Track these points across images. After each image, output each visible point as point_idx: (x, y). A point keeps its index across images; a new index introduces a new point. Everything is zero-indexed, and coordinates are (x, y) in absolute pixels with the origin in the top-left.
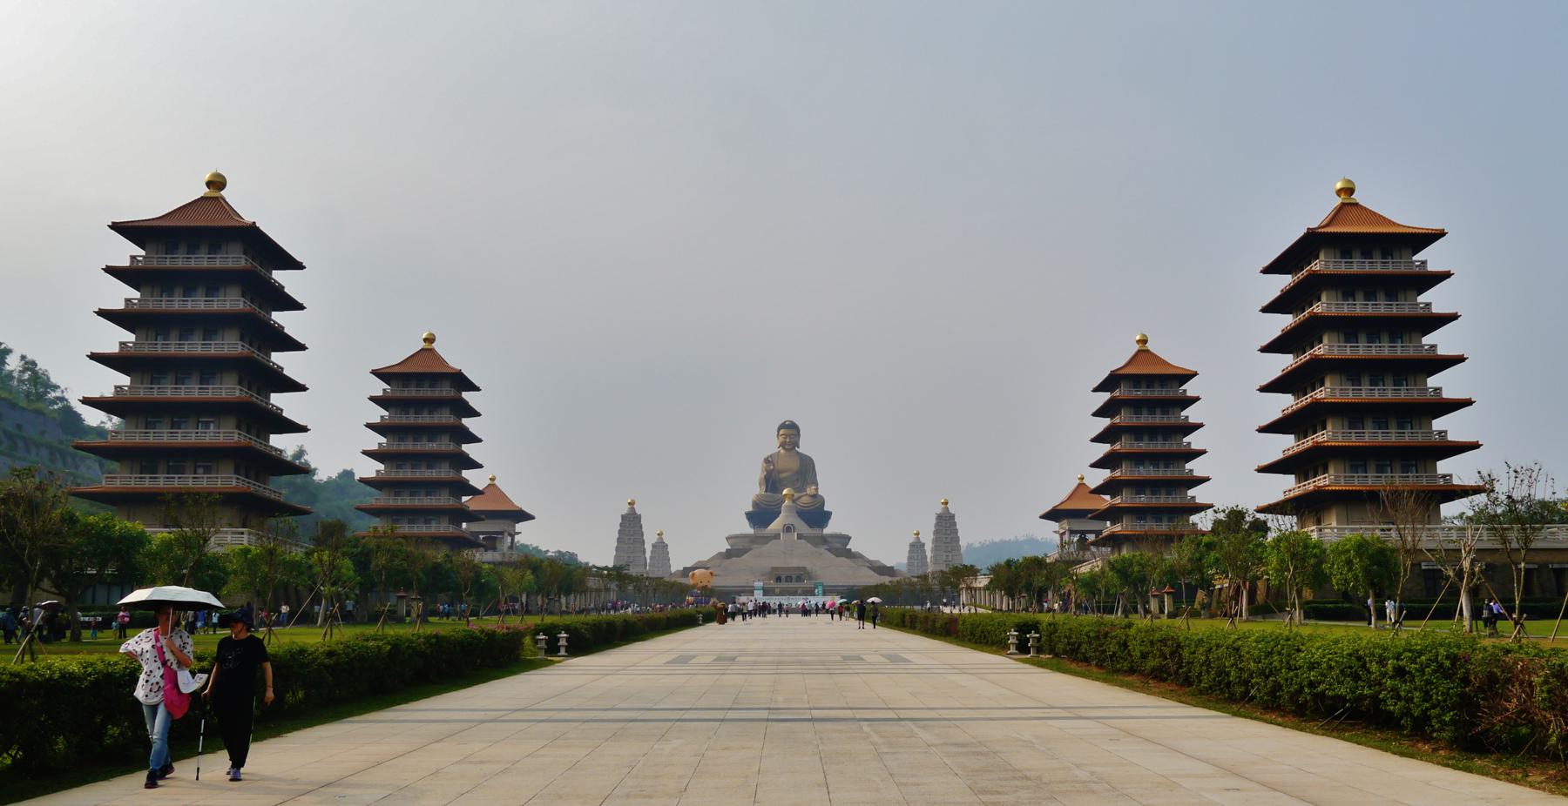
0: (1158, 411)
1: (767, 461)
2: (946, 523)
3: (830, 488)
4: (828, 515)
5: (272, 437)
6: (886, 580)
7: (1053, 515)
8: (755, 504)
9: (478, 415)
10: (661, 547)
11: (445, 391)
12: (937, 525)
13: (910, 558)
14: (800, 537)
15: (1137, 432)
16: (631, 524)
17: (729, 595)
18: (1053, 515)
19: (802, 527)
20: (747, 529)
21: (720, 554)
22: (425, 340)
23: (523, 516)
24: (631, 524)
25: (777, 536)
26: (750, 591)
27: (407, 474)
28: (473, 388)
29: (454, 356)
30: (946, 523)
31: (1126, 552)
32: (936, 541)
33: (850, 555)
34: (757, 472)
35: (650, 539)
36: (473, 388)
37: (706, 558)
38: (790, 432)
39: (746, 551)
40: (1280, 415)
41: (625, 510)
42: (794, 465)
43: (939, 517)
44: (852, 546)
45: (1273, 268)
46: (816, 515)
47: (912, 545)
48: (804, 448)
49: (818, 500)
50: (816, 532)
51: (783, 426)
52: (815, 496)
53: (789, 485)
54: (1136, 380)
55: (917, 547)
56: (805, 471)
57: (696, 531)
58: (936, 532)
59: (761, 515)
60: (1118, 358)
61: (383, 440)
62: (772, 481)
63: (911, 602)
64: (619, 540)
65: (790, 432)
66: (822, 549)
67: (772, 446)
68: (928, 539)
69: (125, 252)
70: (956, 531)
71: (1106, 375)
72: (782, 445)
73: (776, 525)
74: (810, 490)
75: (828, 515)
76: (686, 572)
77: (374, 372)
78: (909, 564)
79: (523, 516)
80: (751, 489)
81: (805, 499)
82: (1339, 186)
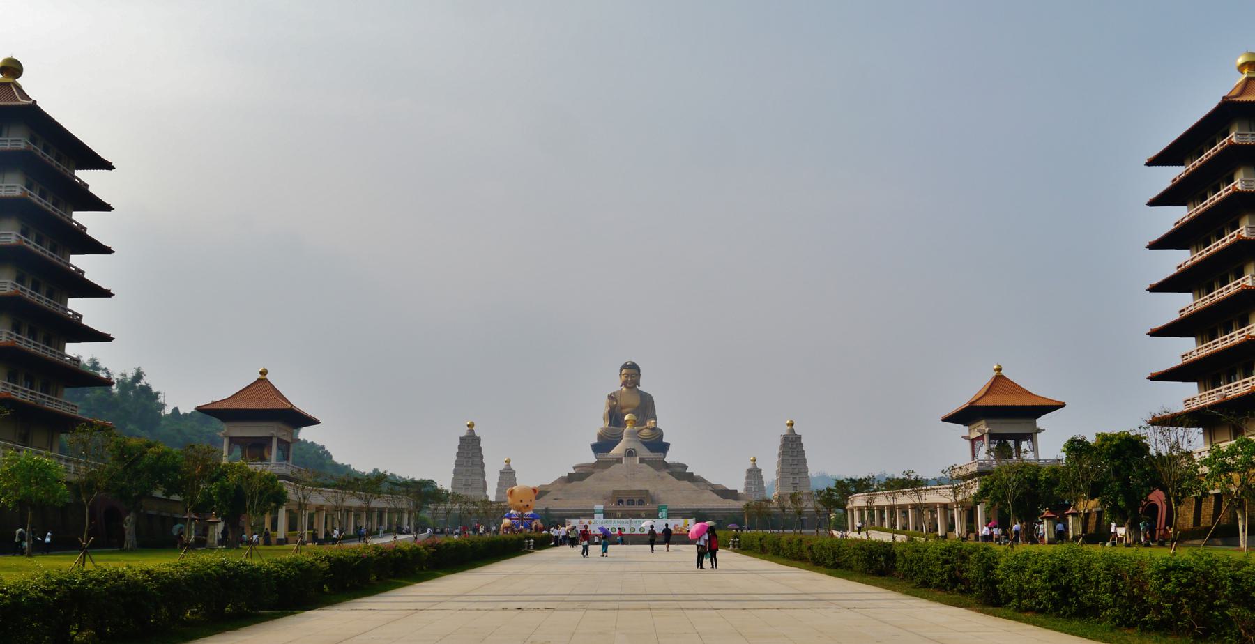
1: (611, 397)
2: (792, 446)
3: (667, 421)
7: (964, 416)
8: (600, 437)
14: (642, 461)
17: (557, 519)
18: (964, 416)
19: (645, 453)
20: (591, 458)
21: (562, 478)
25: (619, 461)
26: (590, 514)
30: (792, 446)
33: (691, 477)
34: (603, 408)
37: (548, 482)
38: (632, 372)
39: (587, 475)
40: (1177, 316)
41: (464, 432)
42: (636, 401)
45: (1162, 159)
47: (749, 471)
48: (644, 386)
50: (657, 456)
51: (625, 366)
52: (654, 429)
55: (754, 474)
56: (646, 407)
57: (539, 453)
59: (603, 445)
62: (615, 416)
63: (796, 526)
65: (632, 372)
66: (665, 473)
70: (803, 453)
71: (1219, 100)
72: (625, 384)
73: (618, 450)
74: (650, 423)
80: (597, 423)
81: (645, 432)
82: (1241, 60)
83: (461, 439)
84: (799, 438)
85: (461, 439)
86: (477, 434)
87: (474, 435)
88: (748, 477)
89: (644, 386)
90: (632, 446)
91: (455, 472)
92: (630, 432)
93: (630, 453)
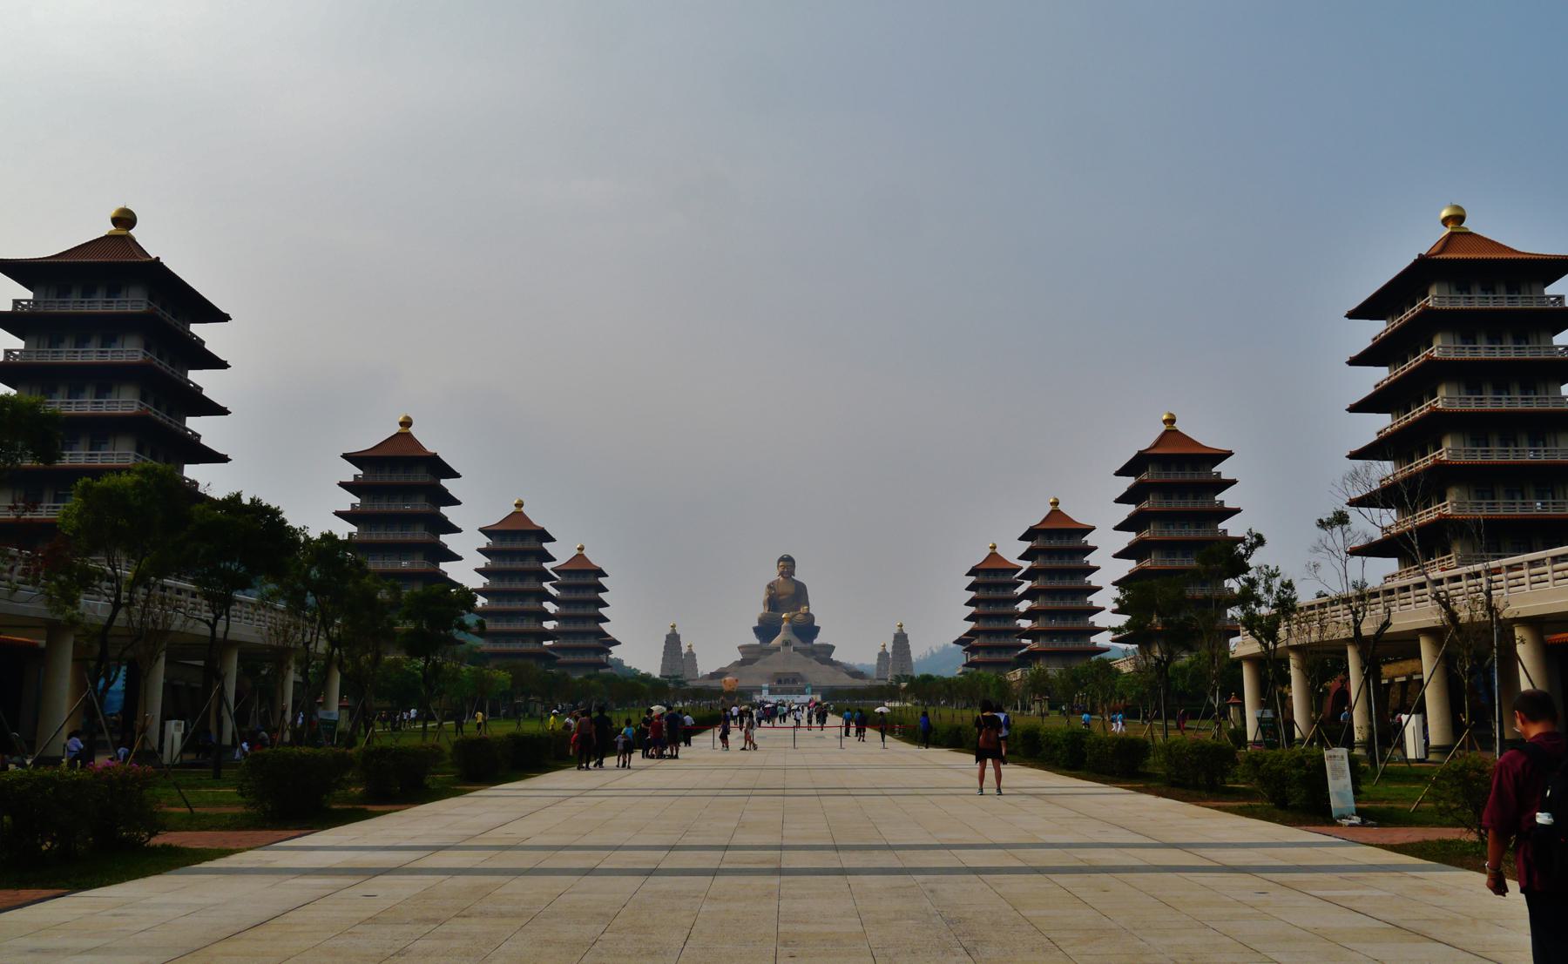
2: (901, 640)
3: (819, 607)
4: (818, 629)
6: (858, 683)
8: (760, 621)
9: (458, 503)
10: (691, 655)
15: (988, 602)
16: (673, 640)
19: (798, 643)
20: (754, 640)
23: (616, 643)
24: (673, 640)
25: (778, 649)
26: (760, 691)
27: (571, 627)
30: (901, 640)
31: (981, 671)
34: (762, 596)
35: (685, 650)
38: (787, 564)
42: (790, 589)
43: (896, 636)
44: (834, 657)
46: (807, 630)
48: (798, 577)
49: (810, 618)
50: (809, 645)
53: (787, 606)
54: (988, 572)
55: (883, 655)
56: (800, 594)
59: (766, 629)
60: (979, 558)
62: (774, 601)
65: (787, 564)
66: (811, 659)
67: (774, 575)
68: (889, 649)
69: (484, 541)
72: (781, 574)
73: (777, 641)
74: (803, 609)
75: (818, 629)
76: (713, 676)
77: (345, 456)
79: (616, 643)
80: (756, 609)
84: (905, 636)
89: (798, 577)
93: (786, 643)
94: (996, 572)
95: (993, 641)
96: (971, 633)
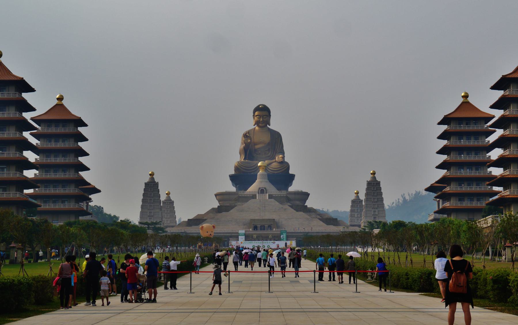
0: (472, 138)
1: (246, 136)
2: (374, 187)
4: (293, 177)
5: (24, 171)
6: (332, 229)
8: (237, 169)
10: (169, 202)
11: (69, 129)
12: (367, 189)
13: (352, 211)
16: (151, 187)
19: (272, 190)
21: (213, 209)
22: (58, 99)
23: (96, 191)
24: (151, 187)
28: (85, 125)
29: (75, 109)
30: (374, 187)
31: (452, 218)
32: (367, 200)
34: (238, 144)
35: (163, 198)
36: (85, 125)
37: (203, 212)
38: (263, 113)
42: (266, 138)
43: (369, 184)
44: (309, 204)
46: (283, 177)
47: (353, 202)
48: (274, 125)
49: (285, 166)
50: (283, 193)
51: (257, 109)
55: (356, 202)
58: (367, 194)
59: (242, 177)
60: (450, 106)
61: (38, 157)
62: (249, 150)
64: (143, 201)
65: (263, 113)
67: (249, 124)
68: (362, 197)
70: (381, 194)
72: (257, 123)
73: (253, 188)
74: (279, 158)
75: (293, 177)
76: (192, 222)
78: (351, 216)
79: (96, 191)
80: (234, 157)
81: (275, 165)
83: (146, 184)
85: (146, 184)
86: (156, 180)
87: (155, 182)
88: (352, 206)
89: (274, 125)
90: (263, 185)
91: (142, 207)
92: (262, 175)
94: (468, 120)
95: (465, 188)
96: (444, 180)
